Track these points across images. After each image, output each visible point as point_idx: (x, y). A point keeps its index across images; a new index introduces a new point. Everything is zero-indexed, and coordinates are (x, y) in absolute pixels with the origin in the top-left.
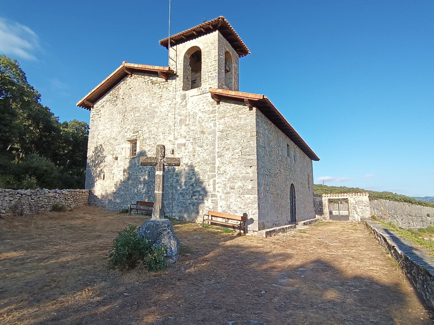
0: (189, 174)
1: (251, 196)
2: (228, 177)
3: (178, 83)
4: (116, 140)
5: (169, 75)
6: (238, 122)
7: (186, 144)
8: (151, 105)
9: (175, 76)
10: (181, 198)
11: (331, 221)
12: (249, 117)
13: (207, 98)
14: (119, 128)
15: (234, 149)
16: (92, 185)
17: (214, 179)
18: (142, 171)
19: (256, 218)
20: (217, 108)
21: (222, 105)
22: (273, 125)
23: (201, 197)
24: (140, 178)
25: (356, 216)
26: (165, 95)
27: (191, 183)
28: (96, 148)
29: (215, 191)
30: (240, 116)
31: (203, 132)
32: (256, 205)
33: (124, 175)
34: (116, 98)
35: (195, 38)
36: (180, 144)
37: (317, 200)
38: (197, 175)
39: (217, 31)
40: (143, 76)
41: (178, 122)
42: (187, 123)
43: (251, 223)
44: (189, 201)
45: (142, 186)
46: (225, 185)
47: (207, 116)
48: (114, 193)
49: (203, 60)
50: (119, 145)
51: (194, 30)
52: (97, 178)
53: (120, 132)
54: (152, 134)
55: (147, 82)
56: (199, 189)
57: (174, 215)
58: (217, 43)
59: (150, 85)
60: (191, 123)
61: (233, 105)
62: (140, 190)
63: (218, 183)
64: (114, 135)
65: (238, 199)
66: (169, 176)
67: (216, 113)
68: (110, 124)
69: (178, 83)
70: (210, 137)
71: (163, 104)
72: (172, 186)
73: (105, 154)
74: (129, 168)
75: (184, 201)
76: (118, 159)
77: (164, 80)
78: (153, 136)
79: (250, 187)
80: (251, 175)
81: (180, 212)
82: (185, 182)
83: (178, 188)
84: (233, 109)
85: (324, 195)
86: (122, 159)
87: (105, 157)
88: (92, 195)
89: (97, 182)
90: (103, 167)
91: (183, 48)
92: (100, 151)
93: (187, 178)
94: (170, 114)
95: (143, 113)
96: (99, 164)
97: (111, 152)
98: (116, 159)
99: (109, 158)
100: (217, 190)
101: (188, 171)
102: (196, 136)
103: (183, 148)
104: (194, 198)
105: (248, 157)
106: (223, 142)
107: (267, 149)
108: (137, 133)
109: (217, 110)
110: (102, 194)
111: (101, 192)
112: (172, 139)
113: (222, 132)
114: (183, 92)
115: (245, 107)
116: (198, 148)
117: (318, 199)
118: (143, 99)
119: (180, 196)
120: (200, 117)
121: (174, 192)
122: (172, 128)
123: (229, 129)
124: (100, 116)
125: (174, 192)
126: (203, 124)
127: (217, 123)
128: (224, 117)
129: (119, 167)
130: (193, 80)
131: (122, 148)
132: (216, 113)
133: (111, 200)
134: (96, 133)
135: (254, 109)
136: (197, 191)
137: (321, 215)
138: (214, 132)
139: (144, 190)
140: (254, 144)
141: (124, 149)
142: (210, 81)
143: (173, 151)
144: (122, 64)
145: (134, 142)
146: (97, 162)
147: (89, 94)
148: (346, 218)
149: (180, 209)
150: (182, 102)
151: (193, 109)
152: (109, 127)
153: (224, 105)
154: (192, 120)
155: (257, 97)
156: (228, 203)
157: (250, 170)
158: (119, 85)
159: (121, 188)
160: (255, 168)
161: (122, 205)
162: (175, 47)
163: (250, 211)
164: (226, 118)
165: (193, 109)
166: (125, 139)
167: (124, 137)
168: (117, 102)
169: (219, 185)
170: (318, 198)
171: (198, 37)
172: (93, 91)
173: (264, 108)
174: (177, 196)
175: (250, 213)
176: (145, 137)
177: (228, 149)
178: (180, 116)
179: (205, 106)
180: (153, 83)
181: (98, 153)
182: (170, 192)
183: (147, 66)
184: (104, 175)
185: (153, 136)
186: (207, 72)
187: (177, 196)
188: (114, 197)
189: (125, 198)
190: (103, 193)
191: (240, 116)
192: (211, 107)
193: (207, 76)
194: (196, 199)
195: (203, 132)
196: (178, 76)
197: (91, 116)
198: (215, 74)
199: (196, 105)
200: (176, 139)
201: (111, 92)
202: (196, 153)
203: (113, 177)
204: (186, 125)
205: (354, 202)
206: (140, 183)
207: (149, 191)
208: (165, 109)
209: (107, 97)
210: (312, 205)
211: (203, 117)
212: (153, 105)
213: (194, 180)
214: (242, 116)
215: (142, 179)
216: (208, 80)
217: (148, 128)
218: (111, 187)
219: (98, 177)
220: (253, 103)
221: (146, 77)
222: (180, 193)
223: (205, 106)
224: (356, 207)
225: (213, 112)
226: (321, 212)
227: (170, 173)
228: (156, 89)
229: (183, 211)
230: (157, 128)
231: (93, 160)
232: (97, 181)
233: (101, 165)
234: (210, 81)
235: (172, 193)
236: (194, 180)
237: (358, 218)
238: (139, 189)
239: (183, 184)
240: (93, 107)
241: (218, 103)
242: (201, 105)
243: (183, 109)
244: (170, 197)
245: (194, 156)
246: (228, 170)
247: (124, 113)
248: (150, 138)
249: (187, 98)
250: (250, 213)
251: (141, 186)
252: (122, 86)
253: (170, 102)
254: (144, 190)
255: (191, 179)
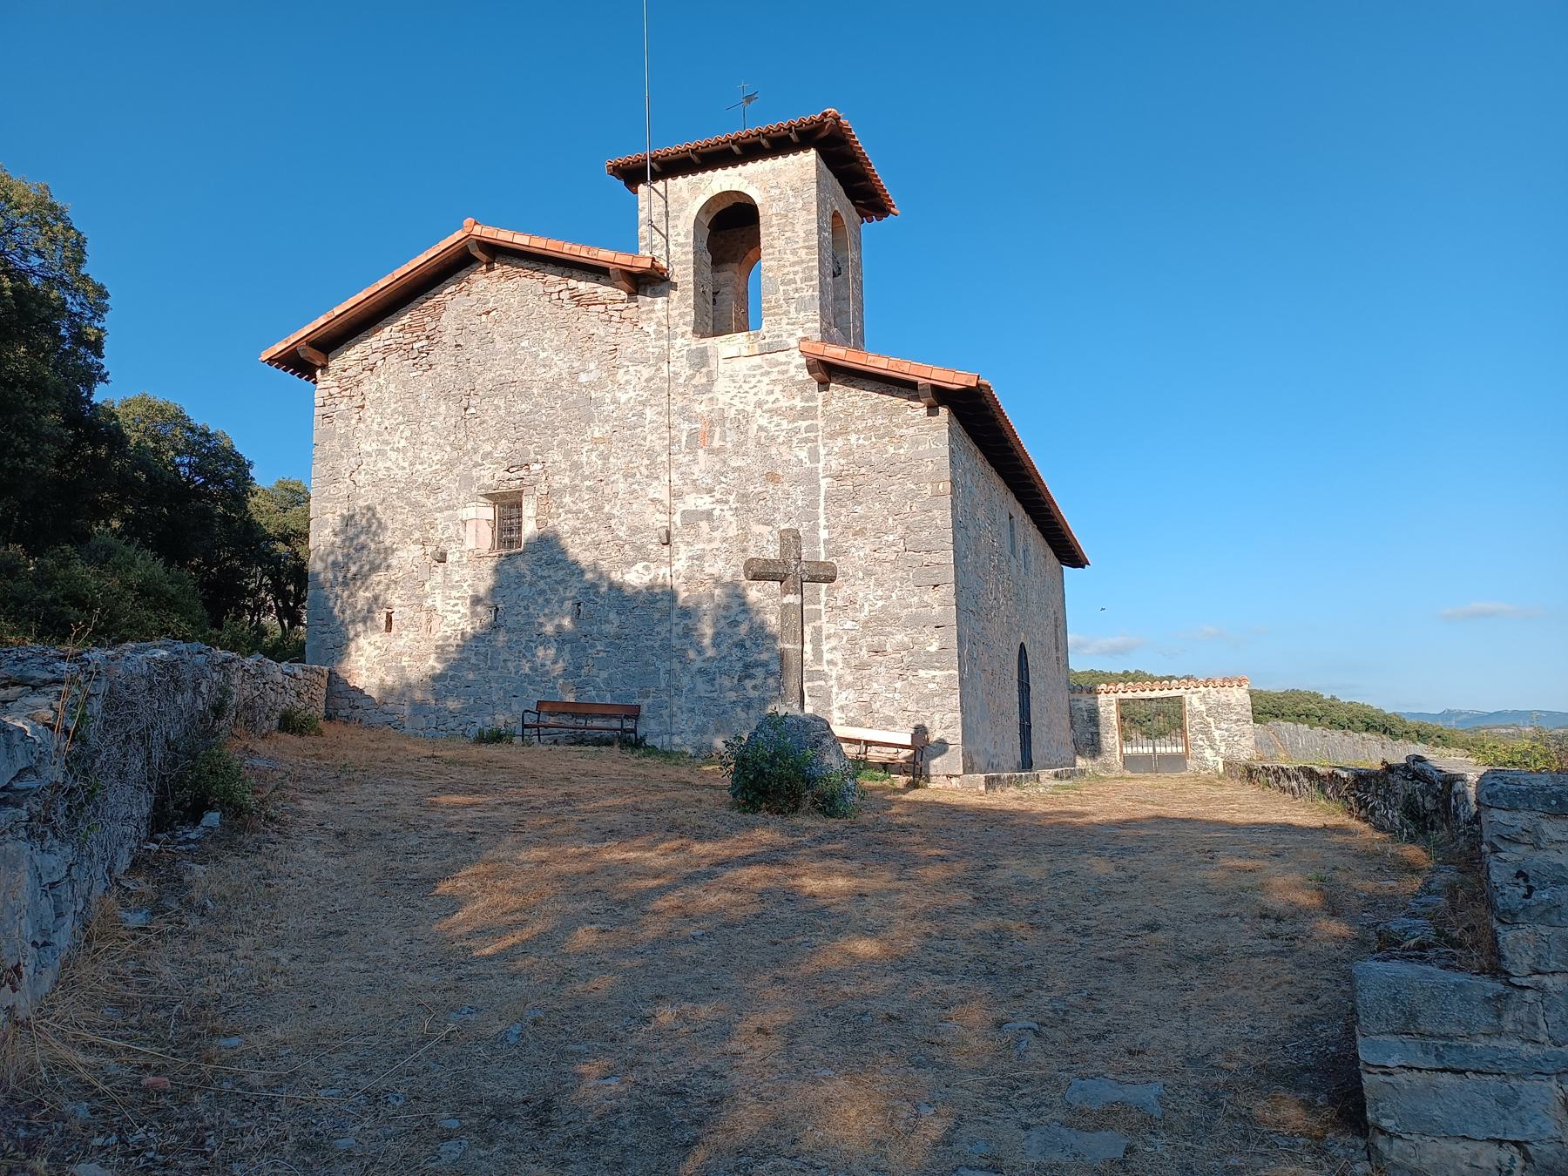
0: (727, 608)
1: (937, 673)
2: (862, 616)
3: (674, 310)
4: (436, 490)
5: (647, 282)
6: (891, 450)
7: (716, 513)
8: (574, 374)
9: (663, 286)
10: (702, 687)
11: (1128, 774)
12: (929, 436)
13: (784, 368)
14: (448, 449)
15: (879, 533)
16: (339, 646)
17: (818, 623)
18: (547, 601)
19: (954, 736)
20: (820, 402)
21: (836, 394)
22: (980, 455)
23: (771, 681)
24: (541, 625)
25: (1209, 753)
26: (629, 345)
27: (736, 639)
28: (348, 520)
29: (821, 659)
30: (899, 432)
31: (773, 478)
32: (955, 700)
33: (474, 614)
34: (425, 342)
35: (734, 165)
36: (692, 513)
37: (1082, 705)
38: (758, 612)
39: (813, 152)
40: (537, 274)
41: (684, 439)
42: (716, 444)
43: (940, 754)
44: (732, 696)
45: (552, 652)
46: (852, 640)
47: (785, 425)
48: (436, 678)
49: (763, 241)
50: (449, 508)
51: (734, 142)
52: (360, 627)
53: (451, 465)
54: (586, 478)
55: (555, 296)
56: (764, 657)
57: (677, 740)
58: (814, 191)
59: (570, 306)
60: (729, 446)
61: (875, 395)
62: (543, 665)
63: (828, 637)
64: (424, 471)
65: (898, 685)
66: (657, 616)
67: (815, 417)
68: (407, 433)
69: (674, 310)
70: (798, 494)
71: (621, 376)
72: (666, 647)
73: (388, 539)
74: (493, 591)
75: (715, 695)
76: (450, 558)
77: (624, 295)
78: (587, 483)
79: (933, 649)
80: (938, 609)
81: (701, 730)
82: (717, 634)
83: (692, 654)
84: (874, 409)
85: (1103, 686)
86: (465, 560)
87: (389, 551)
88: (341, 687)
89: (362, 641)
90: (381, 587)
91: (692, 194)
92: (367, 530)
93: (723, 622)
94: (649, 412)
95: (543, 401)
96: (362, 577)
97: (417, 535)
98: (442, 559)
99: (408, 555)
100: (827, 656)
101: (725, 601)
102: (751, 488)
103: (704, 525)
104: (749, 683)
105: (927, 558)
106: (843, 511)
107: (972, 533)
108: (522, 473)
109: (820, 409)
110: (382, 680)
111: (381, 673)
112: (664, 495)
113: (838, 477)
114: (696, 343)
115: (913, 403)
116: (757, 529)
117: (1084, 701)
118: (542, 355)
119: (699, 680)
120: (761, 428)
121: (677, 666)
122: (659, 459)
123: (863, 470)
124: (358, 401)
125: (677, 666)
126: (773, 451)
127: (822, 451)
128: (844, 432)
129: (453, 587)
130: (725, 306)
131: (464, 523)
132: (815, 417)
133: (423, 703)
134: (345, 464)
135: (944, 411)
136: (758, 664)
137: (1093, 757)
138: (811, 478)
139: (561, 664)
140: (943, 517)
141: (471, 527)
142: (793, 314)
143: (668, 534)
144: (461, 227)
145: (508, 506)
146: (354, 569)
147: (322, 320)
148: (1177, 762)
149: (700, 720)
150: (693, 376)
151: (736, 401)
152: (403, 443)
153: (844, 397)
154: (732, 436)
155: (959, 379)
156: (866, 697)
157: (931, 596)
158: (439, 298)
159: (466, 659)
160: (948, 590)
161: (472, 717)
162: (660, 185)
163: (937, 717)
164: (853, 438)
165: (736, 401)
166: (474, 490)
167: (467, 481)
168: (431, 358)
169: (833, 642)
170: (1085, 697)
171: (744, 162)
172: (337, 311)
173: (975, 416)
174: (686, 680)
175: (937, 724)
176: (556, 486)
177: (861, 533)
178: (689, 419)
179: (777, 394)
180: (577, 299)
181: (357, 536)
182: (663, 666)
183: (567, 246)
184: (389, 616)
185: (587, 483)
186: (783, 283)
187: (686, 680)
188: (436, 693)
189: (484, 692)
190: (389, 680)
191: (899, 432)
192: (798, 399)
193: (780, 295)
194: (755, 687)
195: (773, 478)
196: (674, 286)
197: (318, 402)
198: (810, 292)
199: (746, 387)
200: (676, 495)
201: (406, 319)
202: (752, 542)
203: (429, 621)
204: (711, 452)
205: (1203, 708)
206: (544, 640)
207: (580, 668)
208: (632, 394)
209: (387, 334)
210: (1066, 723)
211: (772, 428)
212: (583, 378)
213: (743, 629)
214: (903, 431)
215: (549, 629)
216: (785, 307)
217: (567, 455)
218: (422, 658)
219: (364, 620)
220: (941, 396)
221: (552, 278)
222: (699, 671)
223: (777, 394)
224: (1208, 725)
225: (806, 413)
226: (1093, 746)
227: (659, 605)
228: (591, 321)
229: (712, 728)
230: (605, 457)
231: (334, 564)
232: (357, 635)
233: (375, 578)
234: (793, 314)
235: (669, 672)
236: (743, 629)
237: (1214, 759)
238: (539, 661)
239: (707, 641)
240: (324, 367)
241: (824, 385)
242: (764, 387)
243: (699, 397)
244: (663, 685)
245: (744, 551)
246: (861, 595)
247: (463, 398)
248: (574, 489)
249: (712, 361)
250: (937, 724)
251: (545, 654)
252: (455, 305)
253: (646, 372)
254: (561, 664)
255: (735, 624)
